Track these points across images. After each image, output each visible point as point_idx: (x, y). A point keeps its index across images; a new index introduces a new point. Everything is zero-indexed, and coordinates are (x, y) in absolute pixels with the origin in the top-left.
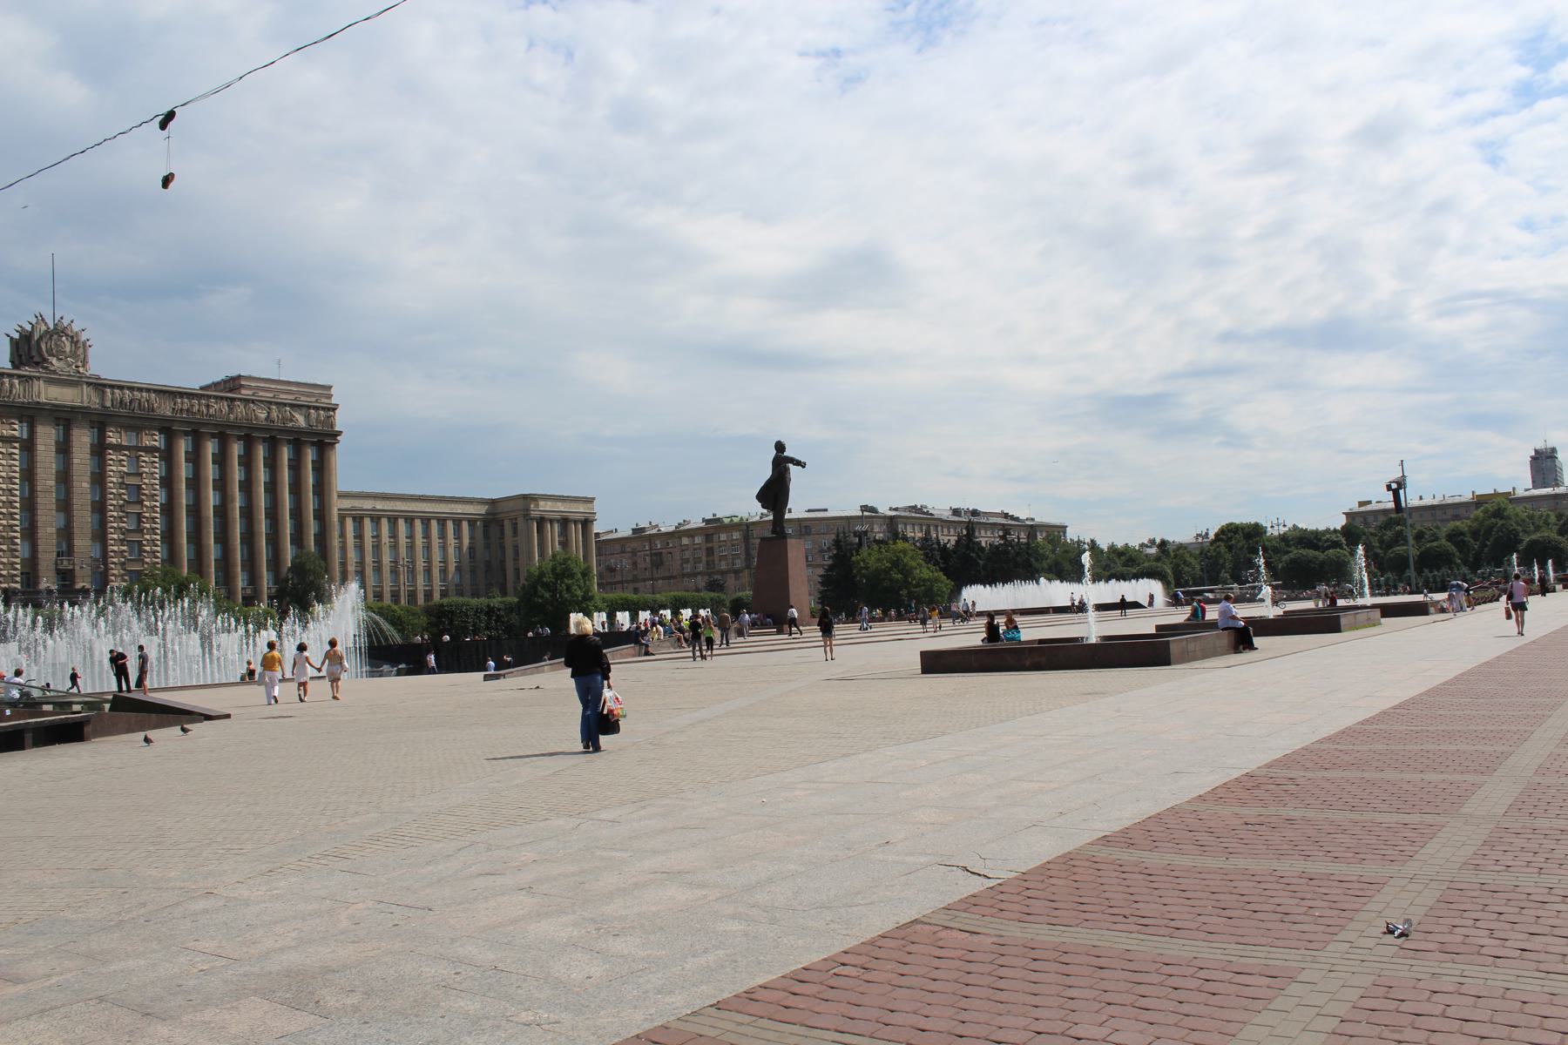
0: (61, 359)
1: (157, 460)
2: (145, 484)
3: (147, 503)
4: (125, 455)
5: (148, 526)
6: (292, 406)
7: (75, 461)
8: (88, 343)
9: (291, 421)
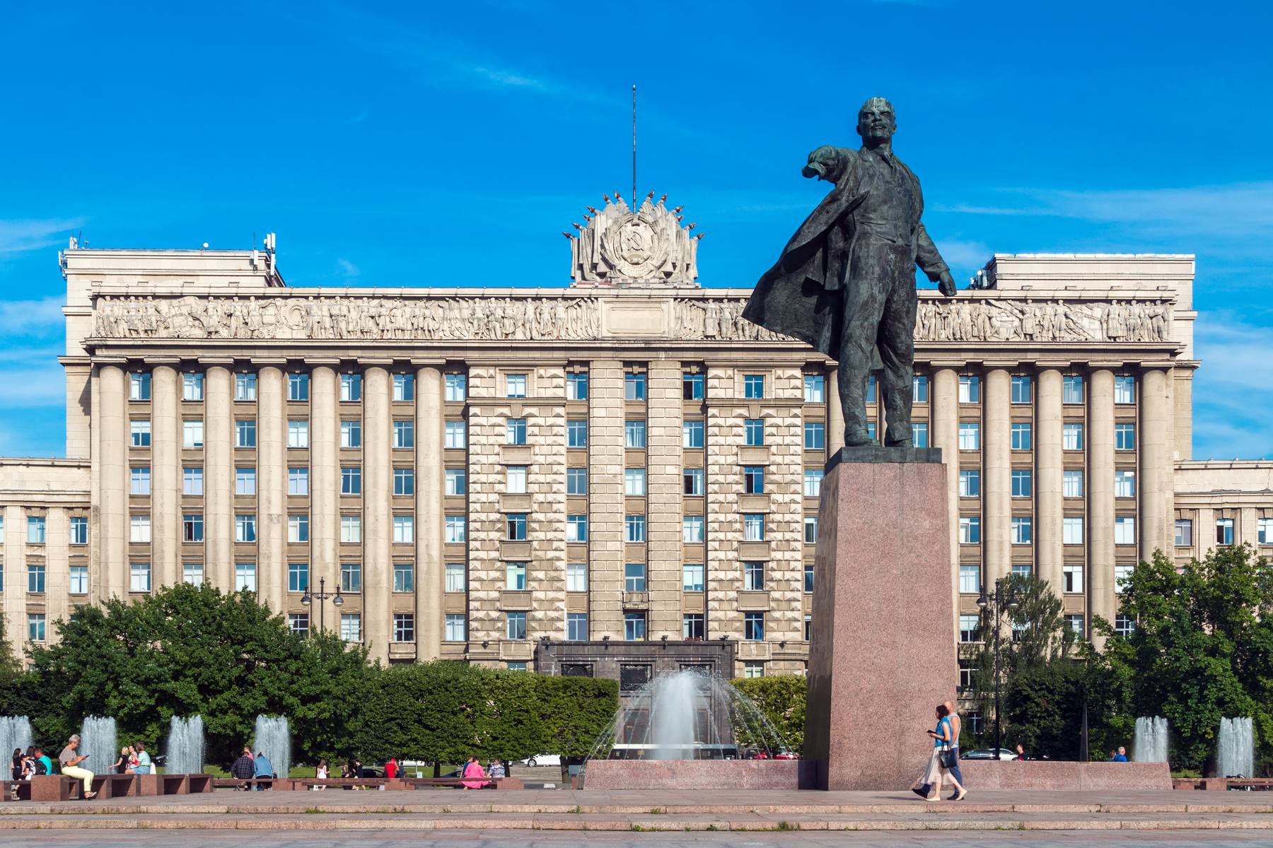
0: (638, 264)
1: (798, 421)
4: (740, 416)
5: (779, 536)
6: (1068, 301)
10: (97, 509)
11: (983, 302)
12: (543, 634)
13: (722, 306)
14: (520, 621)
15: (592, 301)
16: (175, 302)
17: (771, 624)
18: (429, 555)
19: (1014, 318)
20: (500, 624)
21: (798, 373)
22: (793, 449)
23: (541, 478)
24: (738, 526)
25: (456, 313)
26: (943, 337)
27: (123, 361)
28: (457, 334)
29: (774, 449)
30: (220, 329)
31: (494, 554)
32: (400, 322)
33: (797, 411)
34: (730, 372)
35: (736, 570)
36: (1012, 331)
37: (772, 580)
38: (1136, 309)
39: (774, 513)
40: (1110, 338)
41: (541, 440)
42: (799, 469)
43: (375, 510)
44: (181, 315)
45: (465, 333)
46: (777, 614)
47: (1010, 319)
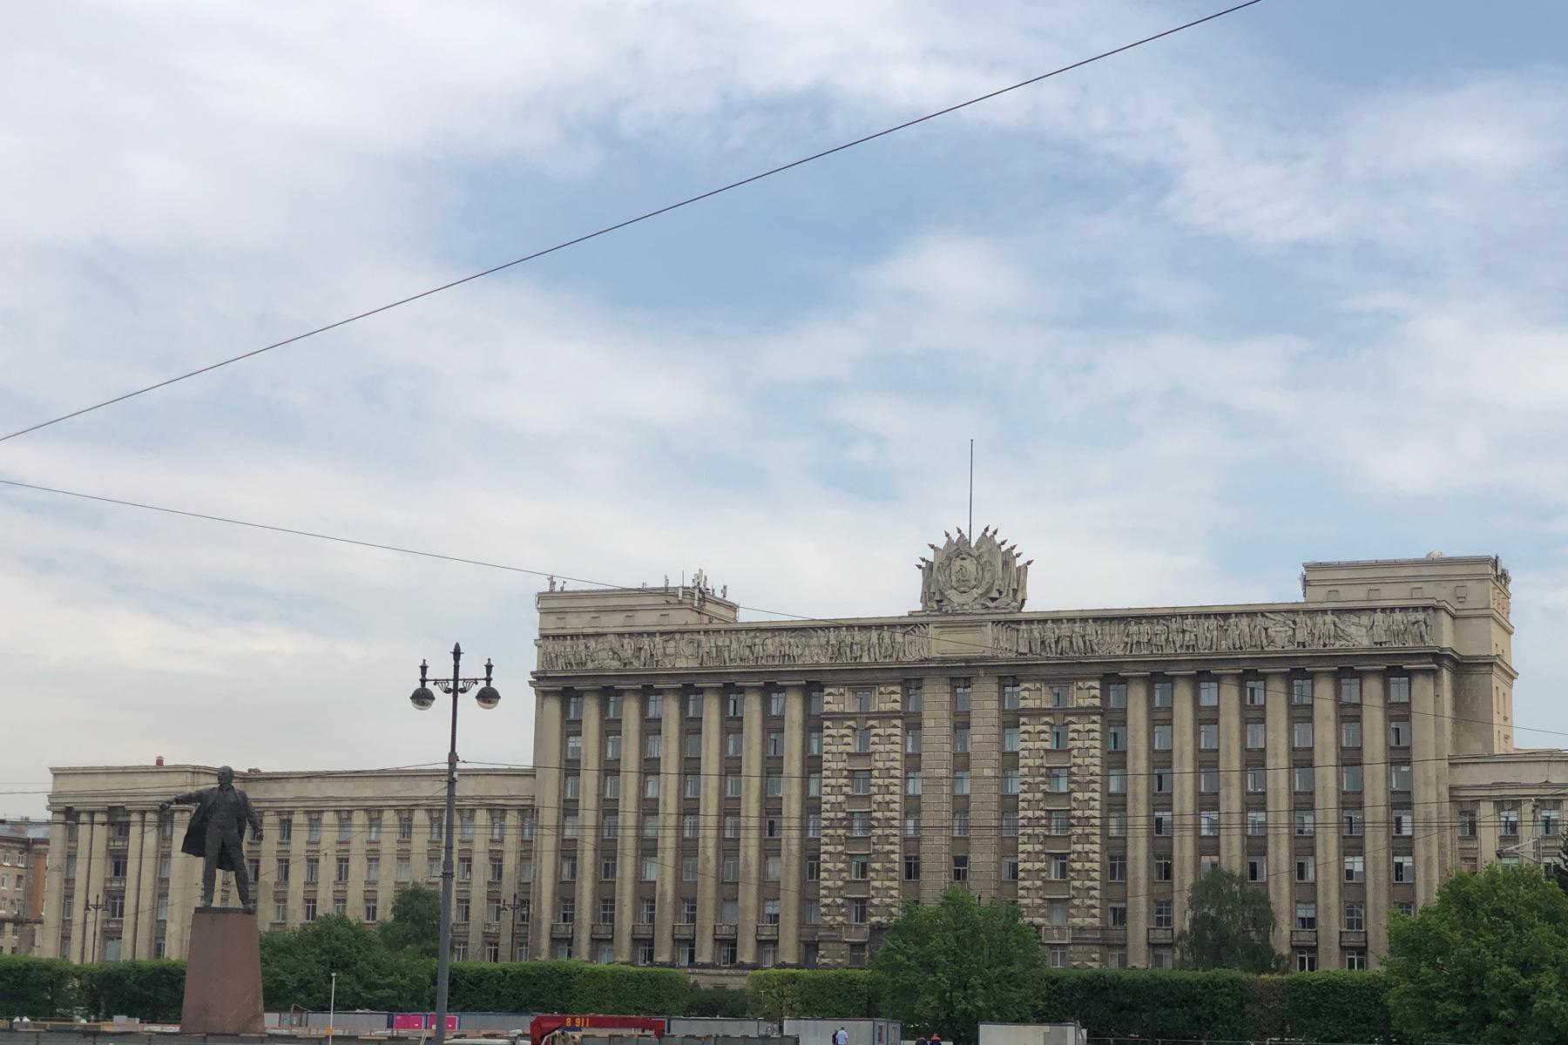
1: (1097, 727)
2: (1075, 765)
3: (1079, 795)
4: (1046, 723)
7: (976, 738)
8: (1020, 562)
9: (1337, 637)
11: (1259, 615)
12: (878, 919)
13: (1033, 627)
14: (862, 907)
15: (925, 628)
16: (600, 640)
19: (1287, 628)
20: (843, 910)
21: (1096, 684)
22: (1092, 751)
23: (880, 782)
24: (1043, 822)
25: (814, 641)
27: (560, 689)
28: (816, 658)
29: (1075, 752)
31: (840, 848)
32: (771, 649)
33: (1094, 718)
34: (1038, 685)
37: (1073, 870)
38: (1398, 616)
39: (1074, 809)
40: (1376, 643)
41: (881, 748)
44: (604, 649)
45: (822, 657)
46: (1077, 902)
47: (1284, 629)
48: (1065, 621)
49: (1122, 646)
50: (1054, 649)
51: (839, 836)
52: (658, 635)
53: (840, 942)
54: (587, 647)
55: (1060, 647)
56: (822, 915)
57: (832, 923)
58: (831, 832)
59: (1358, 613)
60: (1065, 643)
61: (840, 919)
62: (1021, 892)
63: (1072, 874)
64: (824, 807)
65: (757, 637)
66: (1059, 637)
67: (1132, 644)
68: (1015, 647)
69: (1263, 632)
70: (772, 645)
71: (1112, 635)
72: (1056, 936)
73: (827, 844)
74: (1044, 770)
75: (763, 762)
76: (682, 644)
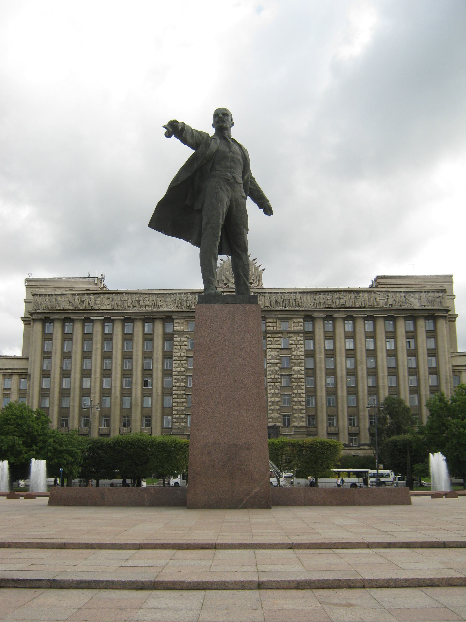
1: (302, 339)
2: (293, 355)
3: (295, 369)
4: (279, 337)
5: (296, 384)
6: (405, 292)
9: (406, 303)
10: (30, 375)
13: (272, 295)
16: (63, 296)
17: (294, 420)
18: (157, 392)
19: (385, 298)
20: (185, 420)
21: (302, 320)
22: (301, 350)
24: (279, 380)
26: (358, 306)
27: (43, 318)
28: (169, 307)
29: (293, 350)
30: (79, 306)
31: (182, 392)
32: (147, 302)
33: (302, 335)
34: (275, 320)
35: (279, 398)
36: (384, 303)
38: (432, 294)
39: (293, 375)
40: (422, 305)
42: (303, 357)
43: (137, 375)
44: (65, 301)
45: (172, 306)
46: (296, 415)
48: (286, 293)
49: (312, 304)
50: (281, 305)
51: (182, 386)
52: (92, 295)
53: (184, 435)
54: (56, 300)
55: (284, 304)
56: (174, 422)
57: (179, 426)
58: (178, 384)
59: (414, 293)
60: (287, 302)
61: (183, 424)
62: (270, 412)
63: (293, 403)
64: (174, 373)
65: (141, 297)
66: (284, 300)
67: (317, 304)
68: (263, 304)
69: (374, 299)
70: (148, 300)
71: (308, 300)
72: (287, 431)
73: (176, 390)
74: (279, 357)
75: (143, 354)
76: (104, 299)
